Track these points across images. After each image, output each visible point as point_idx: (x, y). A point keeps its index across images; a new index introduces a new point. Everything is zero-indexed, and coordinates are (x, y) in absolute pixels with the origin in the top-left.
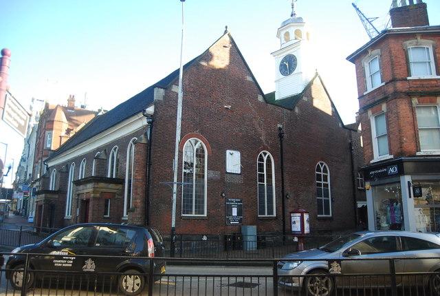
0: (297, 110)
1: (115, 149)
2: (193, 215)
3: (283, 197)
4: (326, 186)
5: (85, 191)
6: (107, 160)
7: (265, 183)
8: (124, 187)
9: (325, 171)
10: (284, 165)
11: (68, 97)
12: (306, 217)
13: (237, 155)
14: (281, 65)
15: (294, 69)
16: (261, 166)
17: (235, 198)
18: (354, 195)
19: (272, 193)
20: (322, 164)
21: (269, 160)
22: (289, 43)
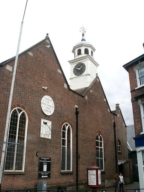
0: (86, 98)
3: (77, 156)
4: (101, 149)
7: (66, 146)
9: (101, 140)
12: (99, 172)
13: (49, 123)
15: (83, 72)
16: (64, 133)
17: (46, 158)
20: (99, 135)
21: (69, 130)
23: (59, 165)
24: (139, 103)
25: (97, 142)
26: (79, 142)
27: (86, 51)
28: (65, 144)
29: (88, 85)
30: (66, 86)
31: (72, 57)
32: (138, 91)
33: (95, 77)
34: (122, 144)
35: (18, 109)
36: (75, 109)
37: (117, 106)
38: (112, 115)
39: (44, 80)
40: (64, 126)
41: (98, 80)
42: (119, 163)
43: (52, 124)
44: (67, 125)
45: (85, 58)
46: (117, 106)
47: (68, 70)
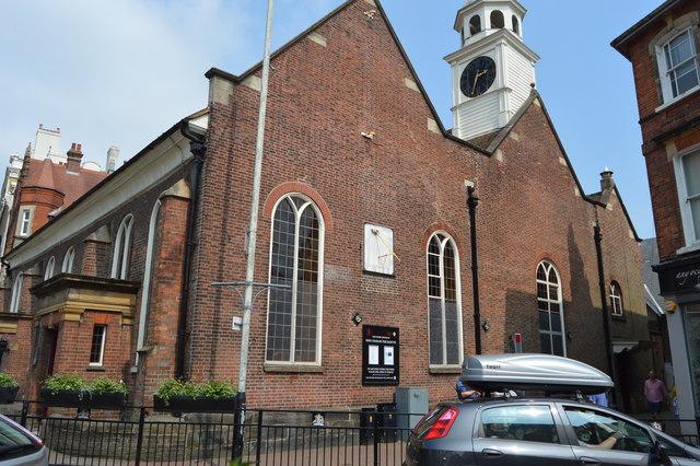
0: (499, 156)
1: (127, 223)
2: (291, 363)
5: (53, 308)
6: (111, 245)
7: (443, 297)
8: (139, 298)
9: (553, 279)
10: (479, 262)
11: (69, 148)
13: (386, 235)
14: (463, 78)
16: (434, 261)
18: (606, 327)
19: (456, 318)
20: (547, 266)
21: (449, 253)
22: (478, 37)
23: (423, 349)
24: (669, 155)
25: (542, 287)
26: (483, 287)
27: (497, 19)
28: (439, 290)
29: (507, 119)
30: (432, 126)
31: (453, 43)
32: (664, 117)
33: (527, 95)
34: (625, 292)
35: (294, 198)
36: (466, 190)
37: (606, 178)
38: (590, 205)
39: (365, 113)
40: (433, 240)
41: (536, 102)
42: (617, 349)
43: (396, 238)
44: (442, 238)
45: (494, 41)
46: (606, 178)
47: (444, 87)
